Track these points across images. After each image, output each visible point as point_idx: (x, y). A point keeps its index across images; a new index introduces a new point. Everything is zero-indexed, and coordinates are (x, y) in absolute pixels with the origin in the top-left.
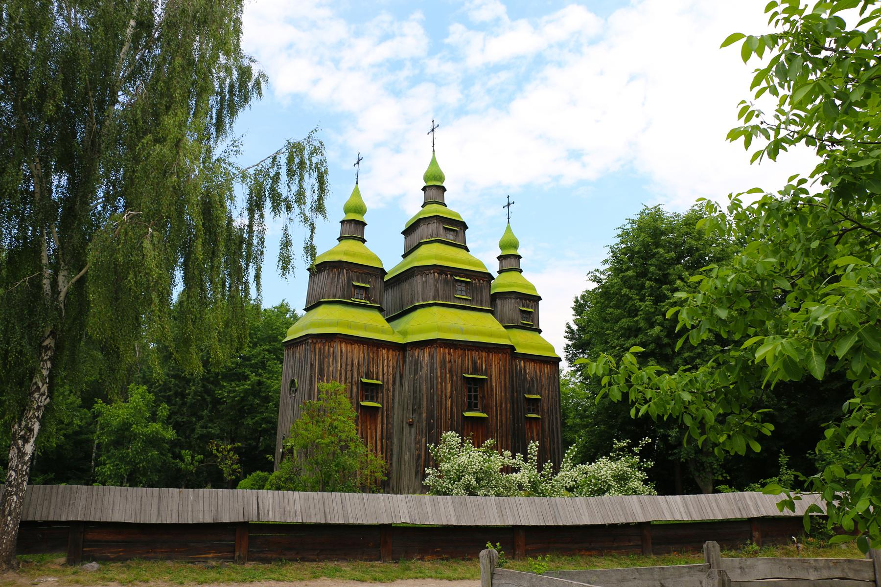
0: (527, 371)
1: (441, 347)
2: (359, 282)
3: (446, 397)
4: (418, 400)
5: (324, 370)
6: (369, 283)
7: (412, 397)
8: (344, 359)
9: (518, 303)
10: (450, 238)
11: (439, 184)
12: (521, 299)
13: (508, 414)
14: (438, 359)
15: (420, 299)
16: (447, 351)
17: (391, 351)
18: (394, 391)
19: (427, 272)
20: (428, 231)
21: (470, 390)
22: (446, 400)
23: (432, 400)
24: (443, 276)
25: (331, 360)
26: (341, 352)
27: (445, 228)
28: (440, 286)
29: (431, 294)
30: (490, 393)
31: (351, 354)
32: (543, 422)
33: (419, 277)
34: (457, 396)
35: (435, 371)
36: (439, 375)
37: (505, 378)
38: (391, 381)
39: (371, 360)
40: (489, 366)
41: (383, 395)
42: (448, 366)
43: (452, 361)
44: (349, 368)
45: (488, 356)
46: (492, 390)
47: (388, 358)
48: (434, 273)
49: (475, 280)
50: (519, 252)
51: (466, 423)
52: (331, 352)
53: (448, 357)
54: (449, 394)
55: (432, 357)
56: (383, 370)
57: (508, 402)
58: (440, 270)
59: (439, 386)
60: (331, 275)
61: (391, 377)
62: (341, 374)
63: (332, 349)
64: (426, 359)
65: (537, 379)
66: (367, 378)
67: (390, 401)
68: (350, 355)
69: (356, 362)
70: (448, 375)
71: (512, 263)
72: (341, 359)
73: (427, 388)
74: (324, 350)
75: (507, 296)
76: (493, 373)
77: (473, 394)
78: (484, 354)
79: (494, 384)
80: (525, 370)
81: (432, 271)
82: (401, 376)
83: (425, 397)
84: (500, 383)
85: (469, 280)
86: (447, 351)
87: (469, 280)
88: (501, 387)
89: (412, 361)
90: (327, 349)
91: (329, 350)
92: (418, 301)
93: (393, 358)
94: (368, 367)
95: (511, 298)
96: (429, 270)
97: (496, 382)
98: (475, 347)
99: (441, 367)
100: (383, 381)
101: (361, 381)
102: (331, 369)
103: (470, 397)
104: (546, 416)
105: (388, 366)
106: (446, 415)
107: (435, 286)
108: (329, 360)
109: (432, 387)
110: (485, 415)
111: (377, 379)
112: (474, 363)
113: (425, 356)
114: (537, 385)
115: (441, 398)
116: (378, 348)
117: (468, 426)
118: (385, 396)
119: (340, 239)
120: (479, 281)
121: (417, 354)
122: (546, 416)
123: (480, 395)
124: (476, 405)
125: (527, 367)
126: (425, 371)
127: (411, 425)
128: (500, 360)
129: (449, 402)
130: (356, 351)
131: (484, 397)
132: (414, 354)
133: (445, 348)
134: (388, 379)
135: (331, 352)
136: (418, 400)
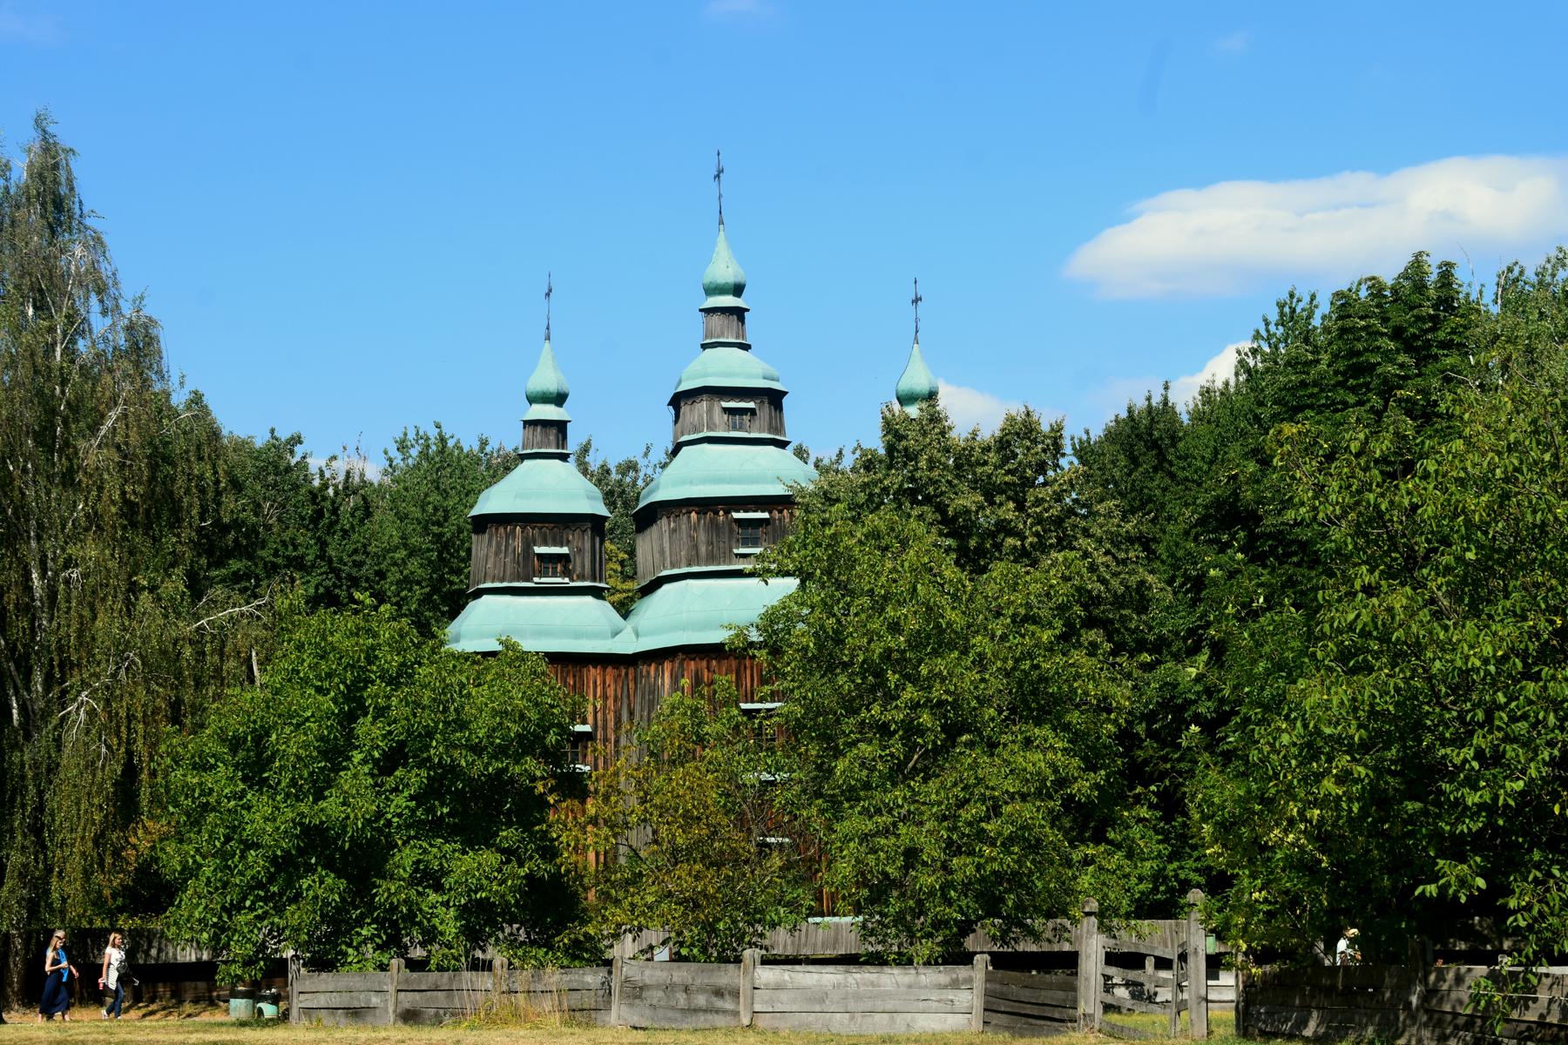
2: (546, 544)
6: (568, 543)
16: (704, 663)
17: (609, 670)
24: (710, 515)
27: (726, 410)
28: (702, 536)
33: (664, 521)
38: (611, 724)
49: (780, 512)
61: (611, 717)
85: (766, 515)
86: (704, 663)
87: (766, 515)
92: (665, 568)
93: (616, 682)
100: (595, 726)
105: (605, 697)
111: (584, 722)
132: (648, 673)
133: (702, 659)
134: (605, 721)
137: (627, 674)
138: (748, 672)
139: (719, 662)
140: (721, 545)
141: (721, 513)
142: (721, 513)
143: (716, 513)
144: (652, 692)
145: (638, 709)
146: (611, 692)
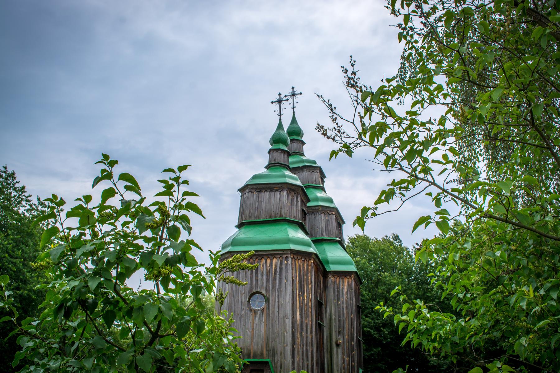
4: (342, 324)
7: (337, 320)
15: (324, 234)
19: (330, 213)
73: (348, 313)
74: (303, 268)
91: (308, 269)
96: (330, 211)
102: (310, 286)
113: (345, 285)
126: (344, 298)
127: (338, 345)
135: (310, 270)
136: (342, 324)
144: (338, 291)
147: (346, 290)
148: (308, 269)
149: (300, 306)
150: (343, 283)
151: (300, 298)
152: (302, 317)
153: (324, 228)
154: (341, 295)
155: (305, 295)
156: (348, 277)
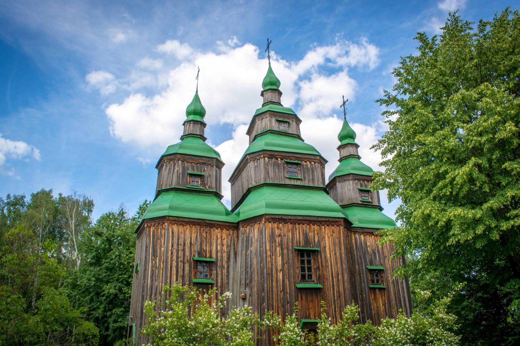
0: (368, 244)
1: (269, 222)
3: (277, 269)
5: (157, 251)
7: (244, 272)
8: (176, 240)
9: (356, 184)
10: (283, 128)
11: (275, 87)
12: (359, 180)
13: (346, 284)
14: (268, 233)
17: (224, 231)
18: (228, 268)
19: (258, 158)
20: (262, 125)
21: (302, 262)
22: (277, 272)
23: (262, 273)
25: (163, 241)
26: (173, 233)
28: (271, 169)
29: (262, 176)
30: (324, 264)
31: (182, 235)
32: (389, 292)
33: (252, 163)
34: (289, 269)
35: (264, 245)
36: (268, 248)
37: (340, 249)
38: (225, 259)
39: (204, 239)
40: (322, 238)
41: (217, 272)
42: (278, 240)
43: (282, 234)
44: (181, 248)
45: (320, 229)
46: (327, 261)
47: (222, 237)
48: (264, 157)
49: (306, 162)
50: (356, 141)
51: (299, 295)
52: (163, 234)
53: (277, 232)
54: (279, 267)
55: (261, 232)
56: (217, 248)
57: (345, 272)
58: (270, 155)
59: (269, 259)
60: (168, 167)
61: (225, 255)
62: (172, 253)
63: (163, 231)
64: (256, 234)
65: (379, 252)
66: (199, 257)
67: (225, 278)
68: (182, 235)
69: (188, 242)
70: (278, 249)
71: (350, 150)
72: (172, 239)
73: (257, 262)
74: (157, 232)
75: (345, 178)
76: (327, 245)
77: (306, 265)
78: (316, 227)
79: (328, 256)
80: (366, 244)
81: (262, 156)
82: (235, 254)
83: (256, 271)
84: (335, 254)
85: (299, 162)
86: (276, 225)
88: (336, 259)
89: (243, 238)
90: (159, 232)
91: (161, 233)
93: (227, 237)
94: (201, 245)
95: (349, 180)
97: (330, 254)
98: (306, 220)
99: (270, 241)
101: (193, 259)
102: (163, 249)
103: (303, 269)
104: (391, 286)
105: (223, 245)
106: (277, 288)
107: (266, 168)
108: (161, 241)
109: (261, 261)
110: (320, 286)
112: (306, 236)
113: (254, 232)
114: (380, 257)
115: (272, 271)
116: (211, 228)
117: (302, 298)
118: (219, 273)
119: (182, 138)
120: (310, 163)
121: (248, 231)
122: (391, 286)
123: (313, 266)
124: (310, 276)
125: (368, 240)
128: (333, 232)
129: (280, 275)
130: (188, 232)
131: (318, 268)
134: (222, 257)
135: (163, 234)
136: (249, 275)
137: (233, 233)
138: (297, 231)
139: (283, 225)
140: (280, 174)
141: (279, 159)
142: (279, 159)
143: (277, 159)
144: (247, 241)
145: (239, 249)
146: (225, 242)
147: (256, 237)
148: (161, 233)
149: (152, 270)
150: (254, 230)
151: (152, 262)
152: (152, 281)
153: (253, 177)
154: (250, 245)
155: (158, 258)
156: (259, 223)
